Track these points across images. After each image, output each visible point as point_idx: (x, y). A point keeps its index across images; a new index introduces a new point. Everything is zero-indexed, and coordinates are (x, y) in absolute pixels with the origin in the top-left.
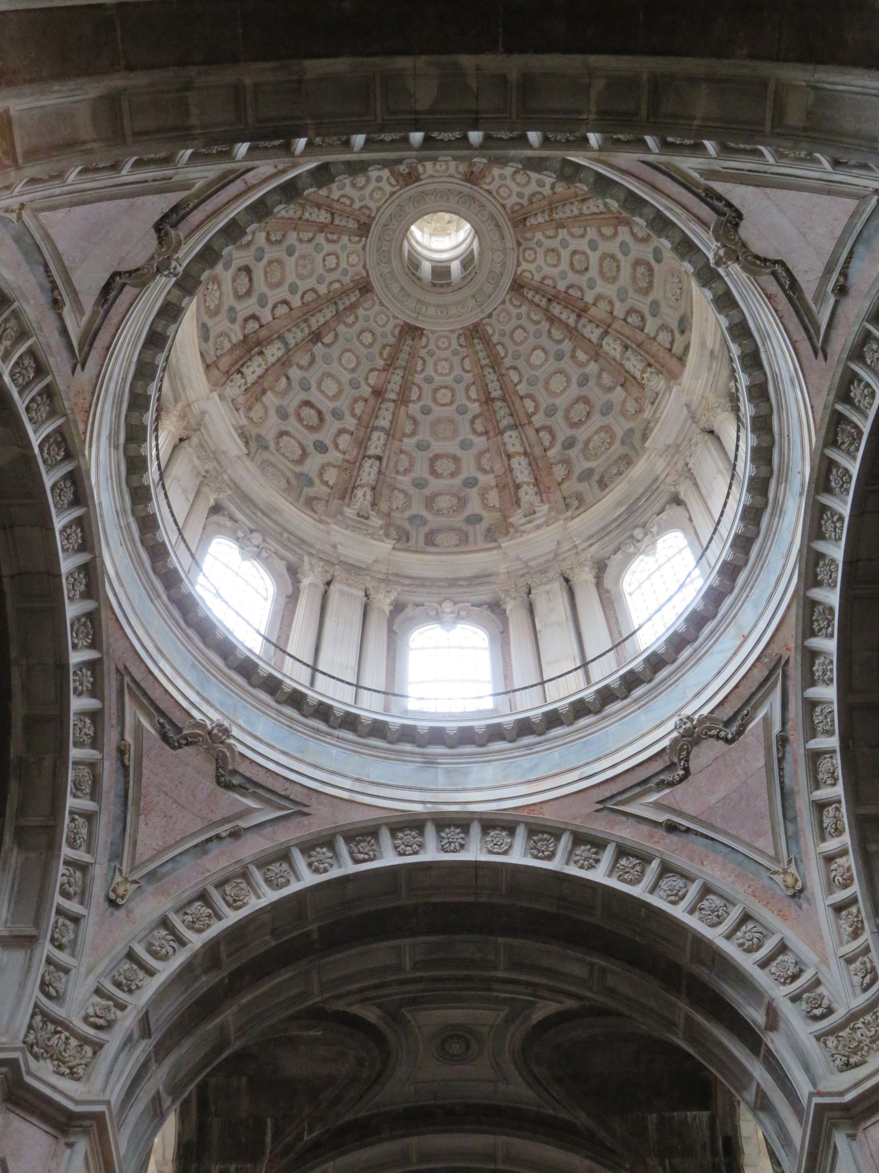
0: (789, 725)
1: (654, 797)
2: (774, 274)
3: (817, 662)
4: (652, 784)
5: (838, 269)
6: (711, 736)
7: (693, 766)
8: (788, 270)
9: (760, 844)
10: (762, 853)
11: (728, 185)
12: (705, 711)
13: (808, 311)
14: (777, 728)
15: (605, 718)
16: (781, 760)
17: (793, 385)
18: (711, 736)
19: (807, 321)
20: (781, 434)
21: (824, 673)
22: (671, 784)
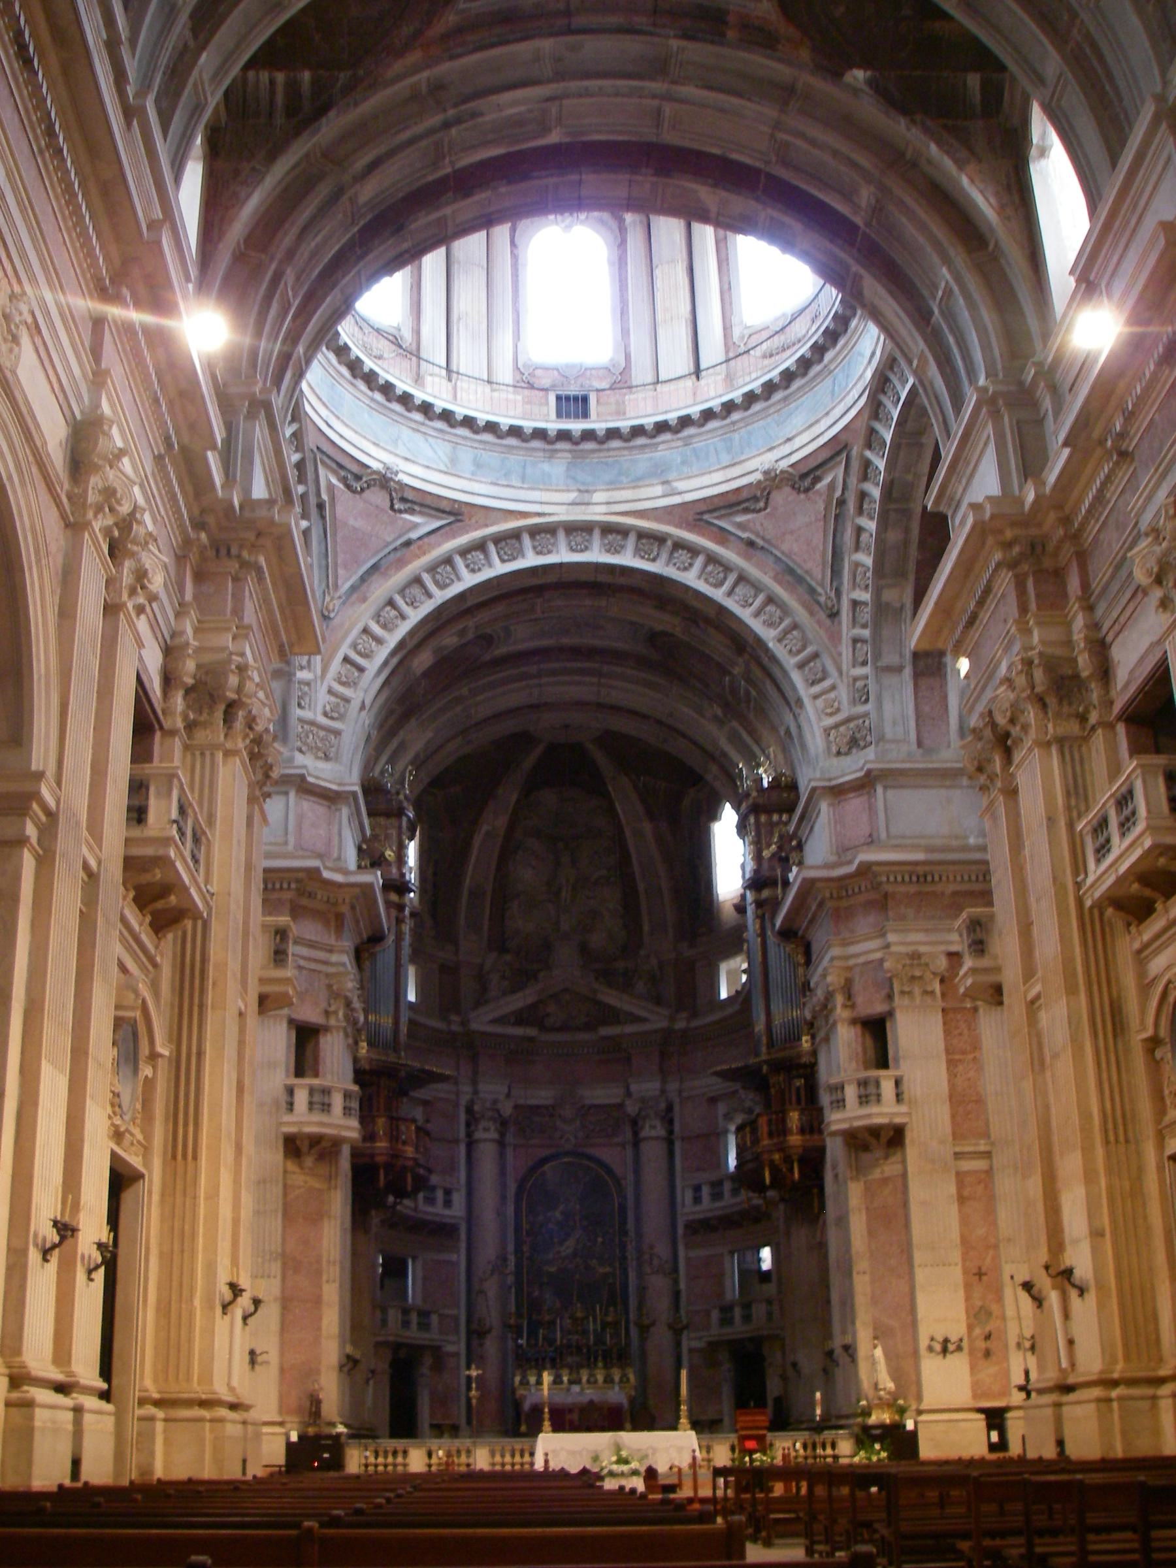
0: (421, 542)
1: (334, 481)
2: (755, 499)
3: (478, 553)
4: (343, 473)
5: (766, 546)
6: (391, 495)
7: (367, 494)
8: (759, 511)
9: (341, 572)
10: (336, 577)
11: (824, 497)
12: (407, 480)
13: (731, 514)
14: (414, 535)
15: (352, 384)
16: (395, 549)
17: (664, 483)
18: (391, 495)
19: (723, 512)
20: (609, 450)
21: (474, 563)
22: (348, 487)
